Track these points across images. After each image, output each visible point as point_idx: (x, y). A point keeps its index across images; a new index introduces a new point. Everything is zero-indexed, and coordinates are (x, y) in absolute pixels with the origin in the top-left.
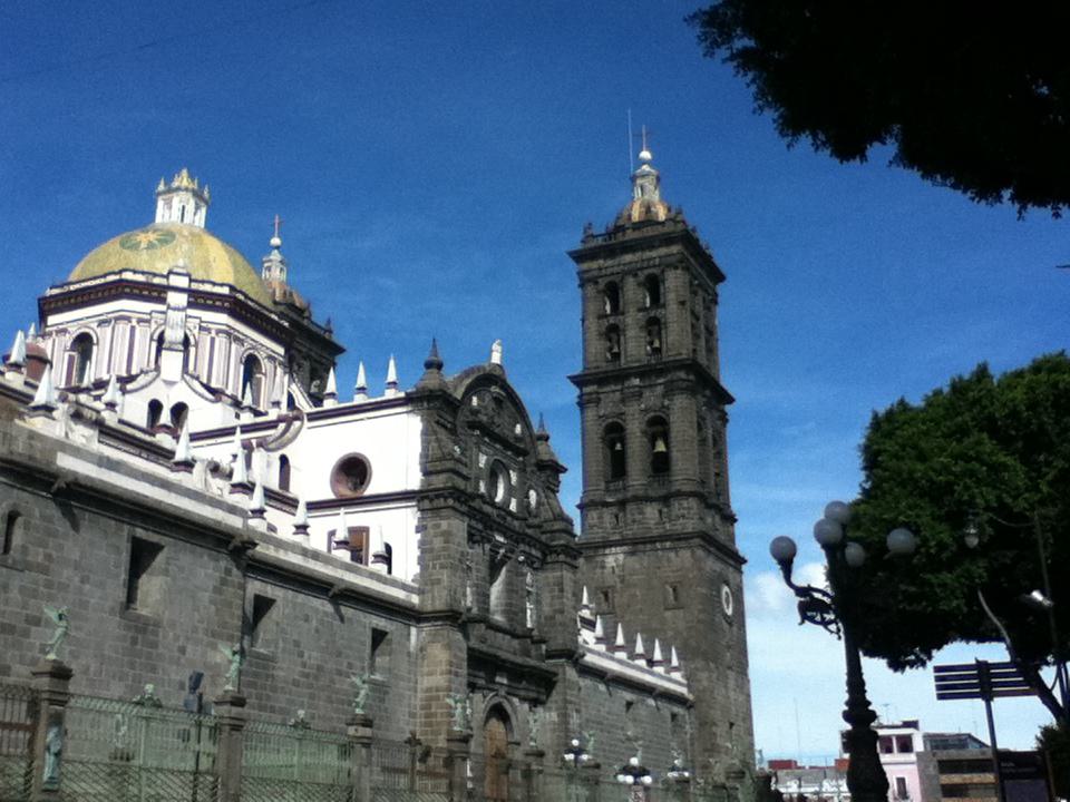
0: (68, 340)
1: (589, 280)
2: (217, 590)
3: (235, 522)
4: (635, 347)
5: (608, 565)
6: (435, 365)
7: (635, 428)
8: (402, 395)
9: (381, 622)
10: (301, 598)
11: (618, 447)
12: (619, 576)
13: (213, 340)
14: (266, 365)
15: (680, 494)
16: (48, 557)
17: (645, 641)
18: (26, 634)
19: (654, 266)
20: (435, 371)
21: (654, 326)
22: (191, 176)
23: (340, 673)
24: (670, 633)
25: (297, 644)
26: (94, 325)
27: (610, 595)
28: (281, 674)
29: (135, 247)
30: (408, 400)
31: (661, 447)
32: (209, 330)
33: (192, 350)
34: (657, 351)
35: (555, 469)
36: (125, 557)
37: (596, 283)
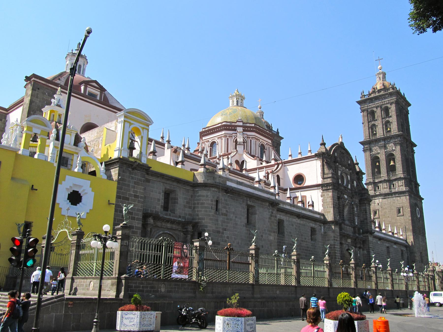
0: (209, 144)
2: (270, 218)
3: (273, 197)
6: (323, 144)
7: (382, 157)
8: (313, 154)
9: (312, 225)
10: (290, 219)
11: (377, 164)
13: (251, 140)
14: (267, 147)
16: (227, 211)
18: (223, 233)
19: (387, 104)
21: (387, 124)
23: (302, 241)
24: (399, 224)
25: (290, 233)
26: (216, 139)
28: (286, 242)
30: (317, 156)
31: (392, 163)
32: (249, 138)
33: (245, 144)
35: (360, 174)
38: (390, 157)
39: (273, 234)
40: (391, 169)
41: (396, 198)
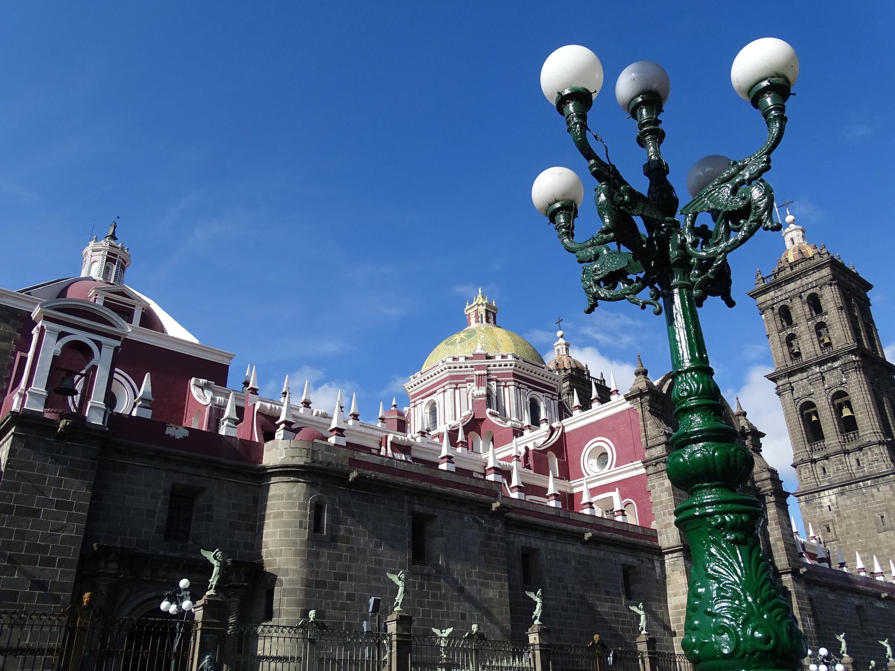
1: (767, 308)
4: (808, 346)
5: (824, 505)
9: (630, 560)
10: (559, 547)
11: (814, 418)
12: (836, 512)
15: (870, 444)
17: (863, 559)
18: (335, 587)
20: (642, 376)
22: (484, 297)
24: (886, 550)
27: (831, 528)
29: (453, 343)
31: (846, 412)
34: (829, 344)
36: (408, 526)
37: (773, 309)
38: (840, 399)
39: (494, 583)
40: (848, 425)
41: (870, 490)
